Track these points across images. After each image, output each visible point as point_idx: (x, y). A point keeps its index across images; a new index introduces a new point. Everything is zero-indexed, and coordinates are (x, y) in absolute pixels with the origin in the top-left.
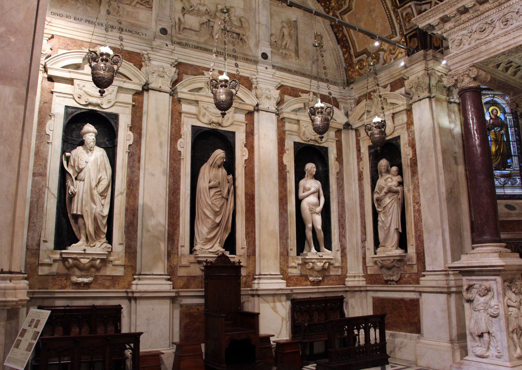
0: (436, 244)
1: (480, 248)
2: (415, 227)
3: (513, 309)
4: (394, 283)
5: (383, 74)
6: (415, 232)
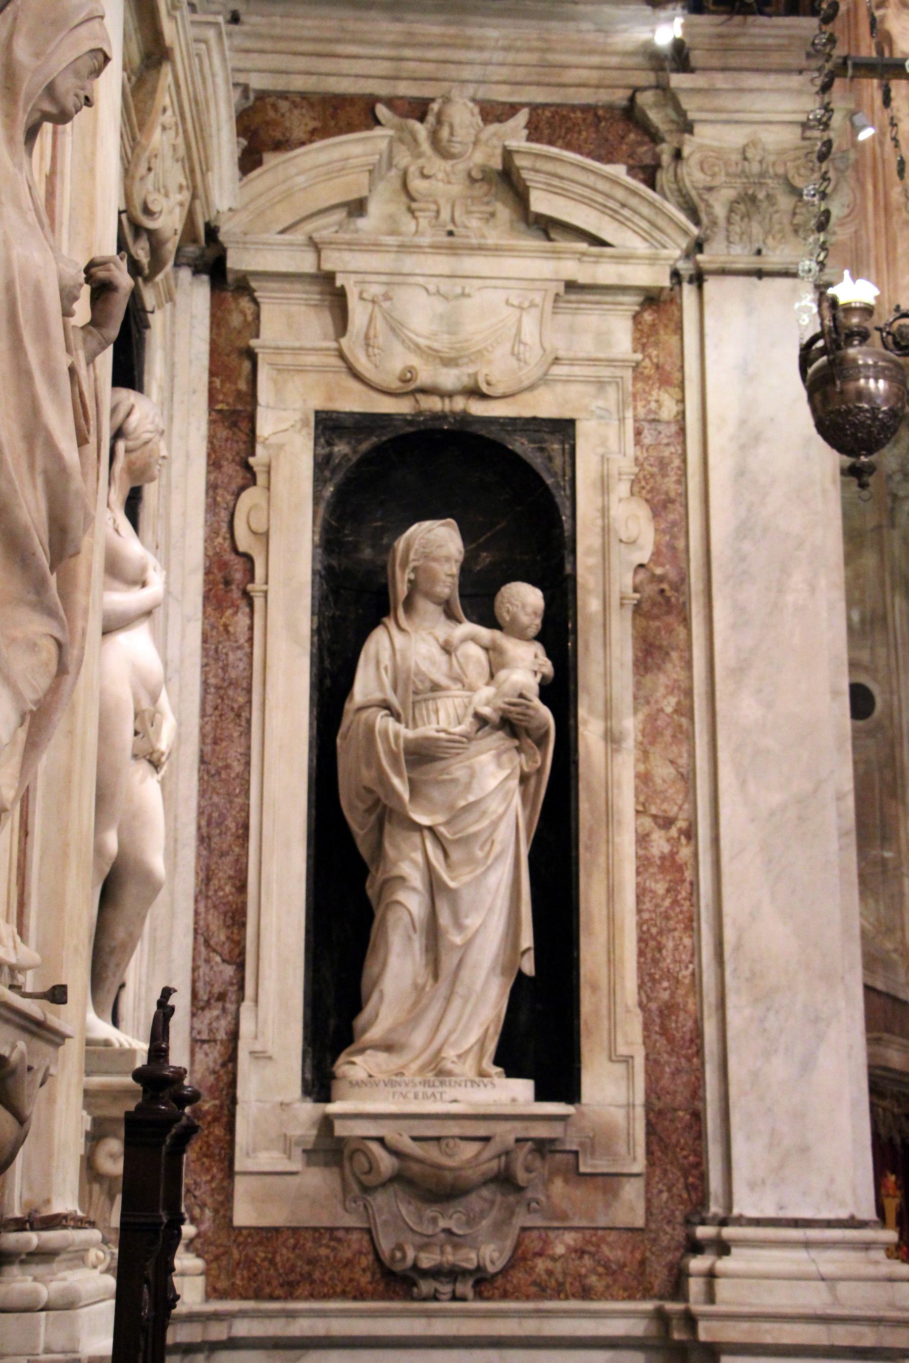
0: (807, 1065)
2: (641, 953)
4: (465, 1287)
5: (492, 33)
6: (640, 987)
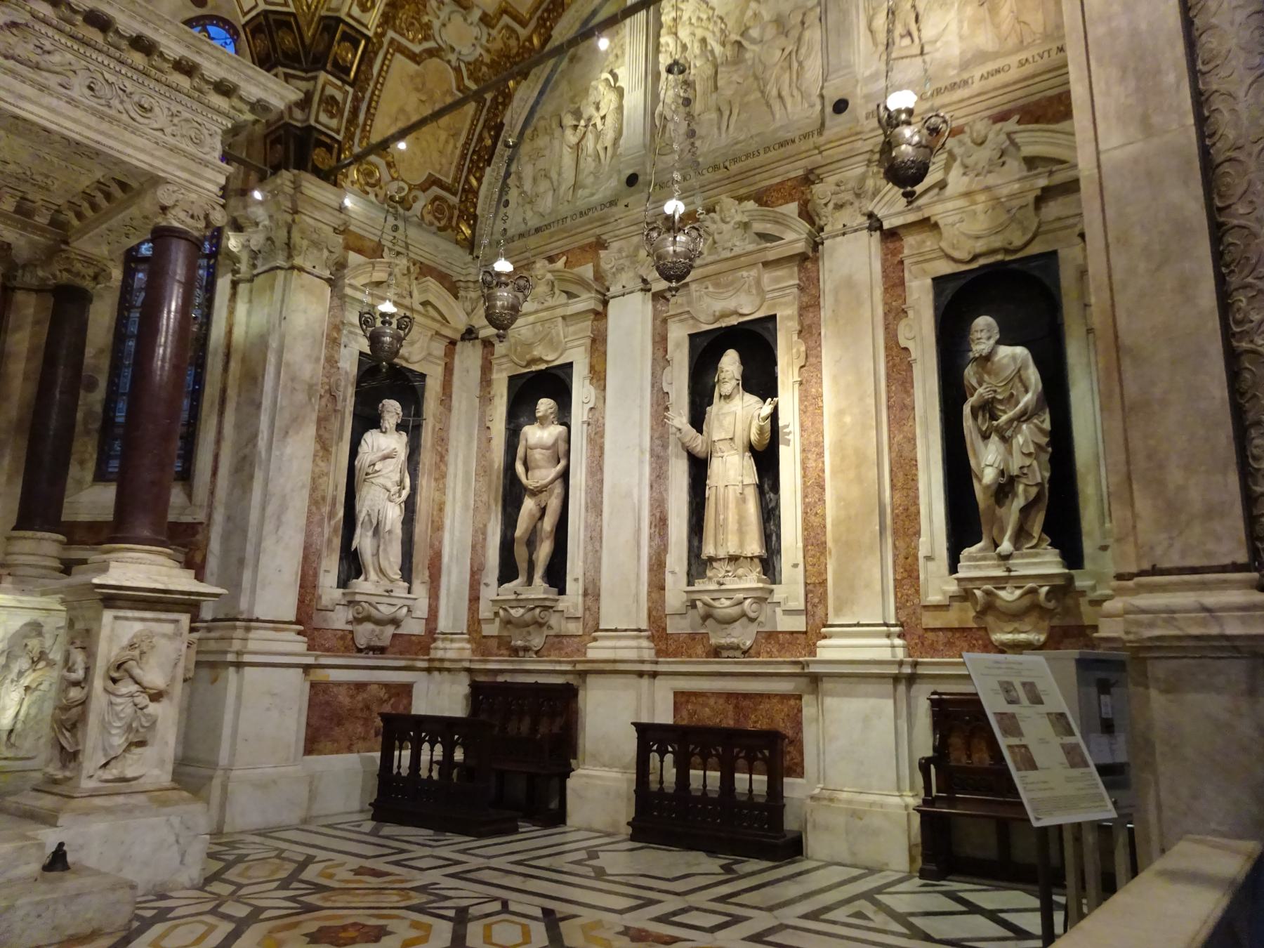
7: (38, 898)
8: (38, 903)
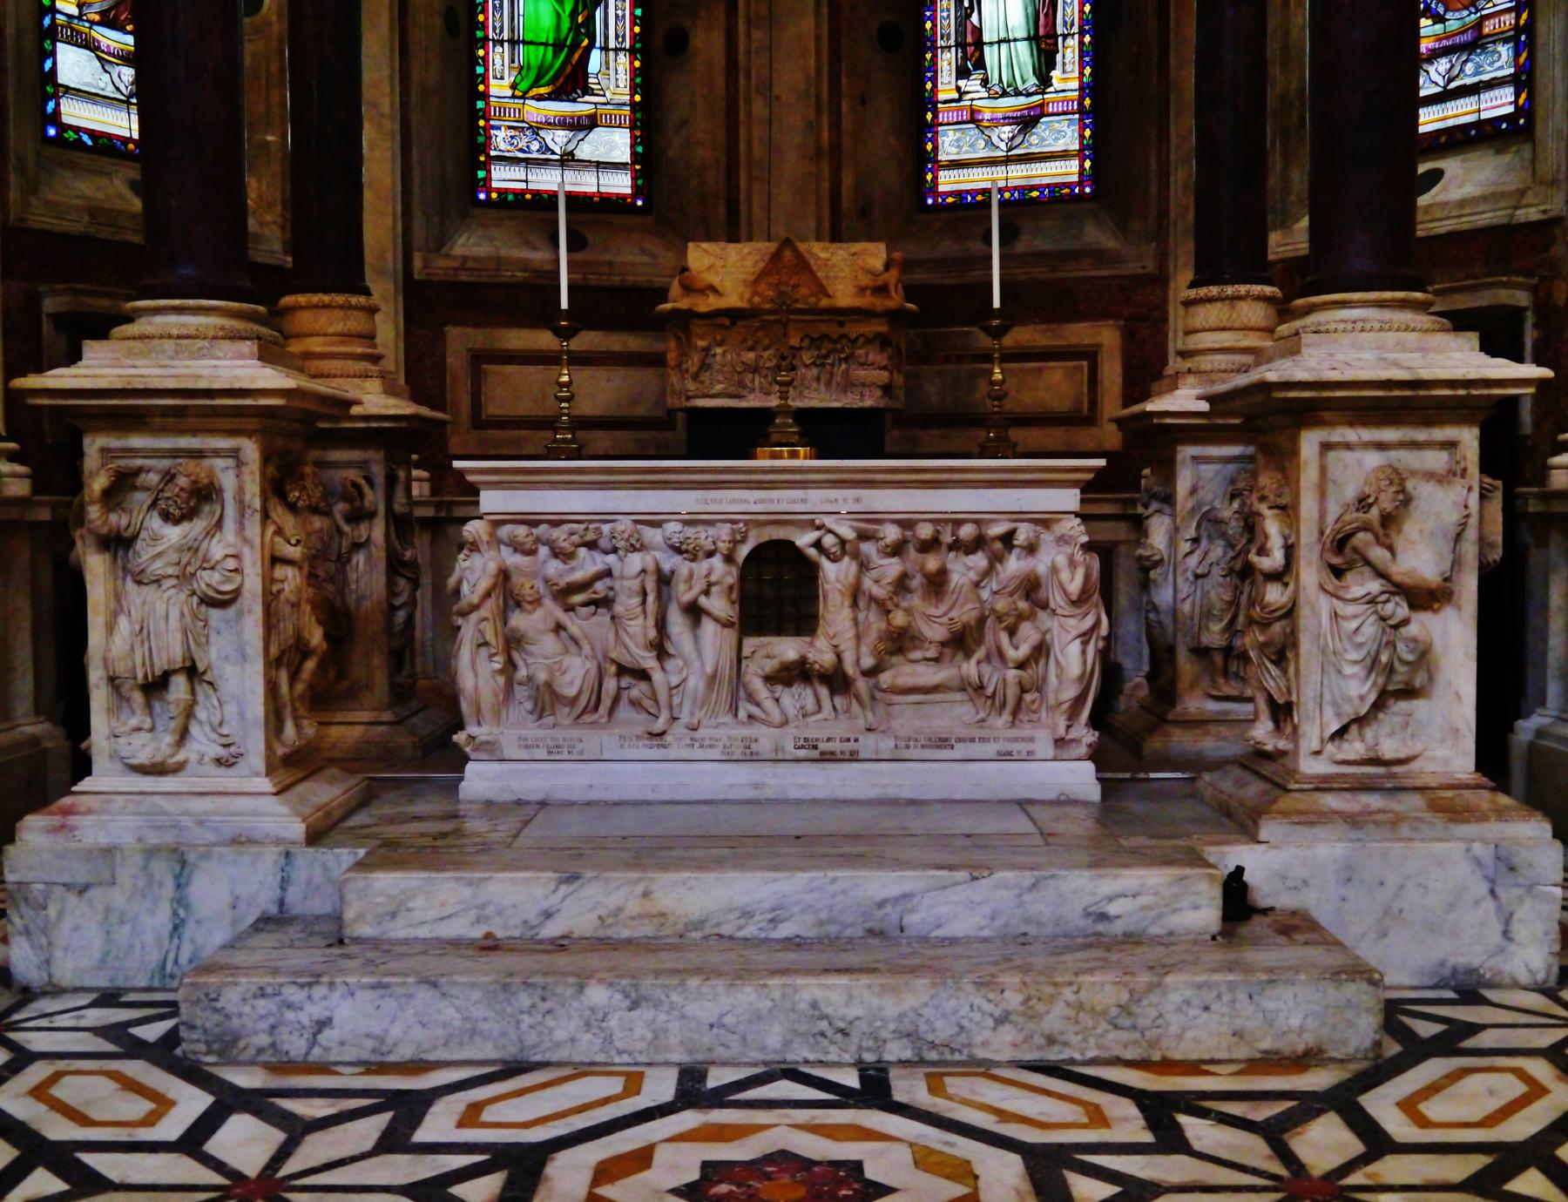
1: (173, 319)
3: (290, 572)
7: (1200, 978)
8: (1199, 987)
